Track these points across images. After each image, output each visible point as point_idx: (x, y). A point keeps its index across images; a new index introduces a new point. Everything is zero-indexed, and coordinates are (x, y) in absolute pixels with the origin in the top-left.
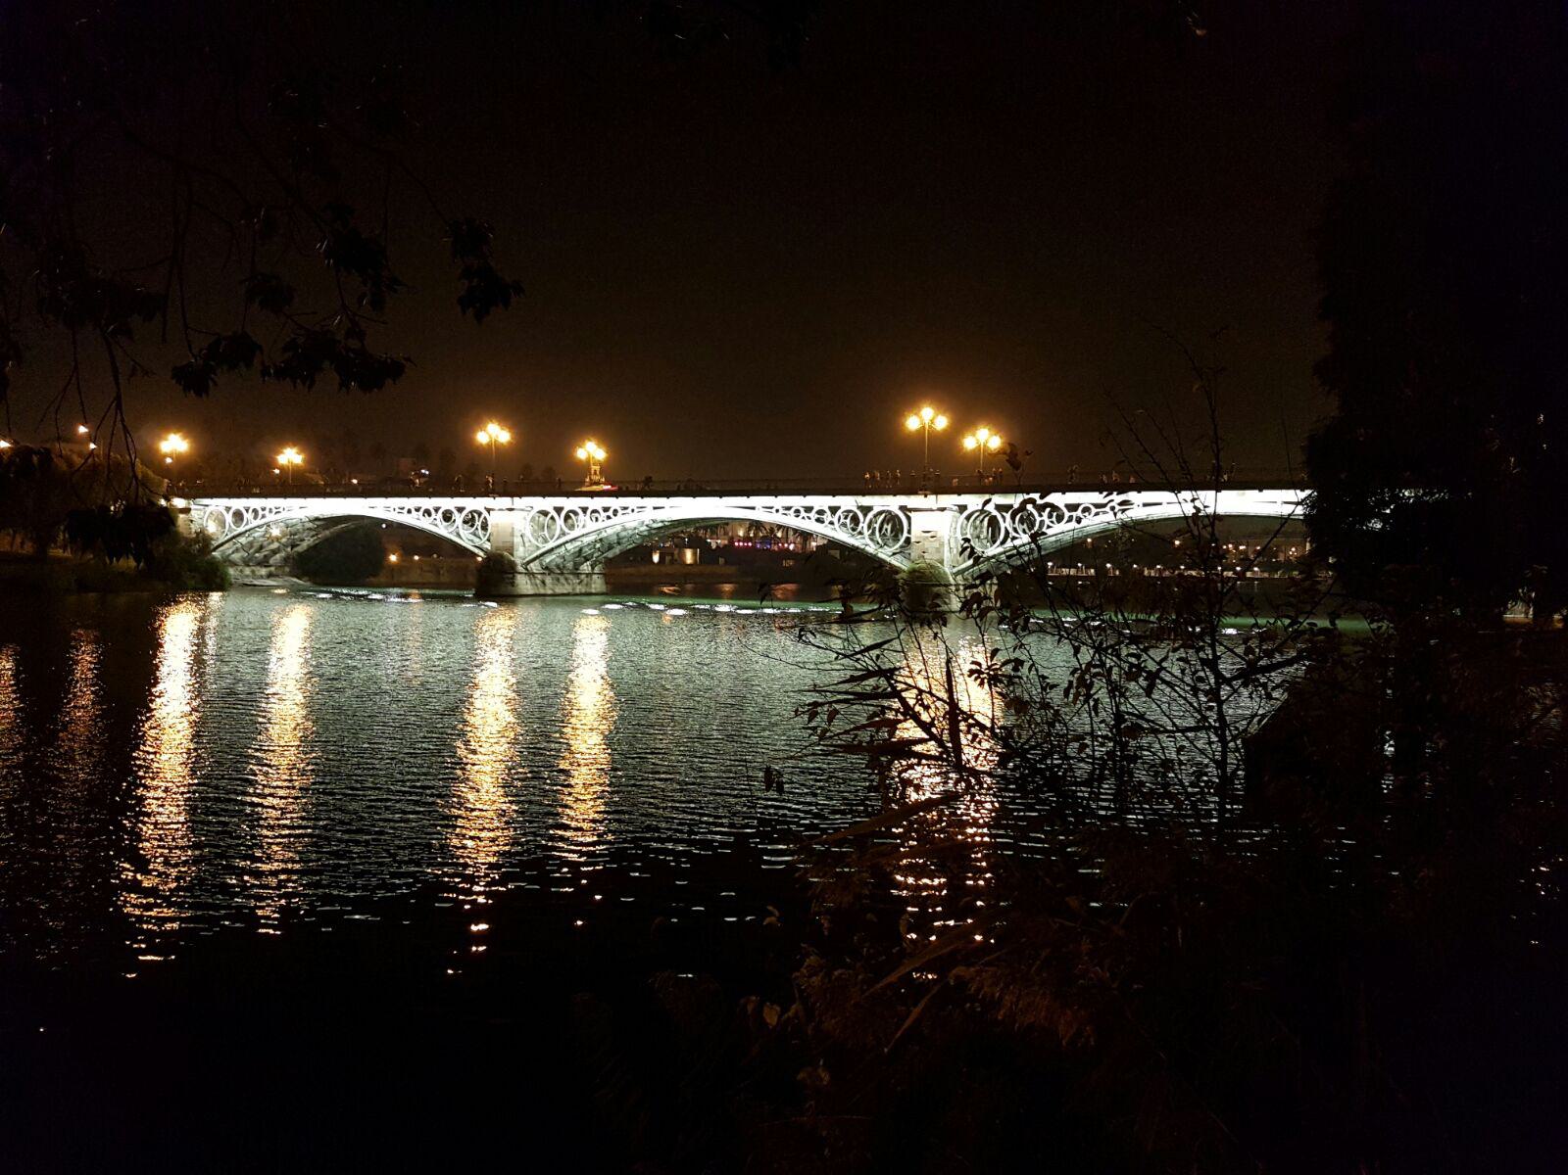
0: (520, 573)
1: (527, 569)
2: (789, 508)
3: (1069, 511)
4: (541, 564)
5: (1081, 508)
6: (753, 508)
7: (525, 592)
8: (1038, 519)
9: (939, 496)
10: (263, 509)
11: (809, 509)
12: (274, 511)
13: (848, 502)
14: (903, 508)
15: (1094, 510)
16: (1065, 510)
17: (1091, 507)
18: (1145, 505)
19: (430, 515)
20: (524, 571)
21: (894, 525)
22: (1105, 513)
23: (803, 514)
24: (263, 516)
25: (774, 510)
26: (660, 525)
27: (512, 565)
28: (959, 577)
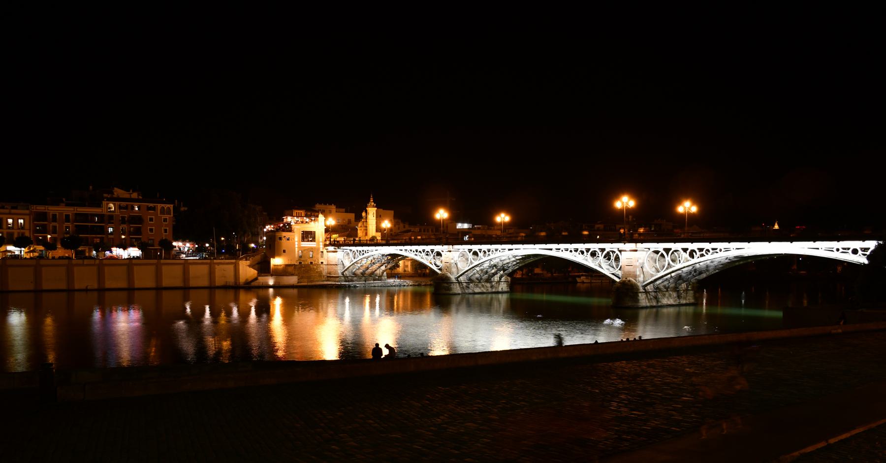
0: (641, 292)
1: (458, 280)
3: (700, 252)
4: (654, 286)
5: (705, 250)
7: (456, 292)
9: (638, 244)
10: (363, 251)
12: (367, 252)
16: (697, 251)
19: (421, 253)
20: (644, 291)
24: (363, 254)
25: (561, 250)
26: (520, 257)
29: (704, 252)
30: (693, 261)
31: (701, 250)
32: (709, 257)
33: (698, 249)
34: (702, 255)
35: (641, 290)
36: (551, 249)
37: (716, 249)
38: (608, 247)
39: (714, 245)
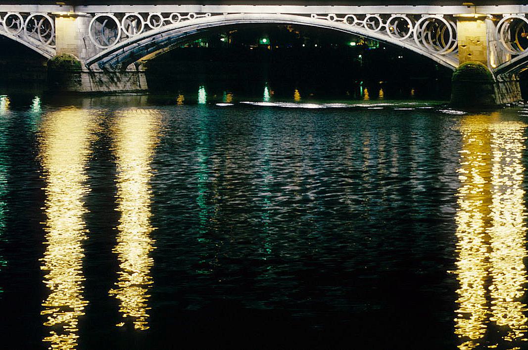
4: (99, 64)
5: (171, 16)
14: (49, 14)
15: (180, 17)
16: (161, 17)
17: (179, 15)
21: (46, 29)
22: (187, 19)
27: (78, 66)
28: (93, 66)
29: (170, 19)
30: (156, 30)
31: (166, 15)
32: (175, 24)
33: (162, 14)
34: (168, 23)
35: (85, 69)
37: (187, 14)
38: (33, 10)
39: (184, 8)
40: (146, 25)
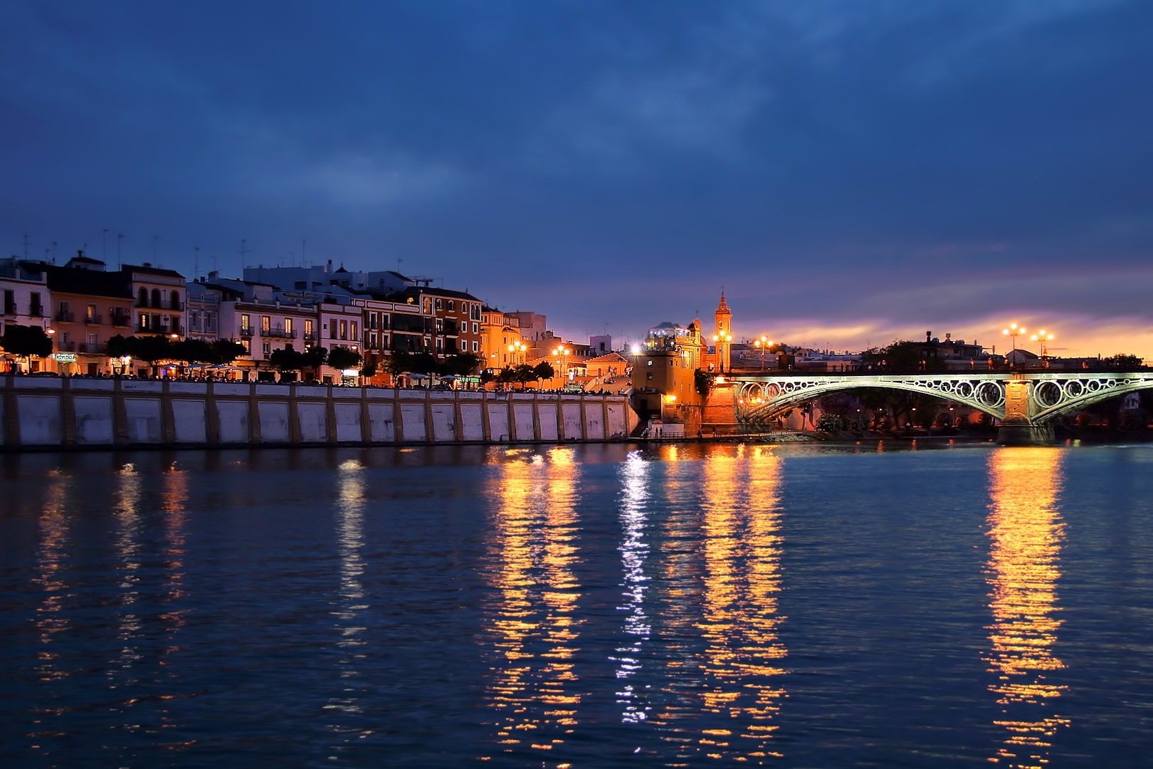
2: (925, 382)
5: (1108, 382)
6: (901, 382)
8: (1083, 388)
11: (937, 383)
13: (964, 378)
14: (999, 382)
16: (1099, 383)
18: (1146, 380)
21: (991, 394)
23: (934, 385)
25: (914, 383)
36: (901, 382)
38: (983, 378)
40: (1085, 389)
